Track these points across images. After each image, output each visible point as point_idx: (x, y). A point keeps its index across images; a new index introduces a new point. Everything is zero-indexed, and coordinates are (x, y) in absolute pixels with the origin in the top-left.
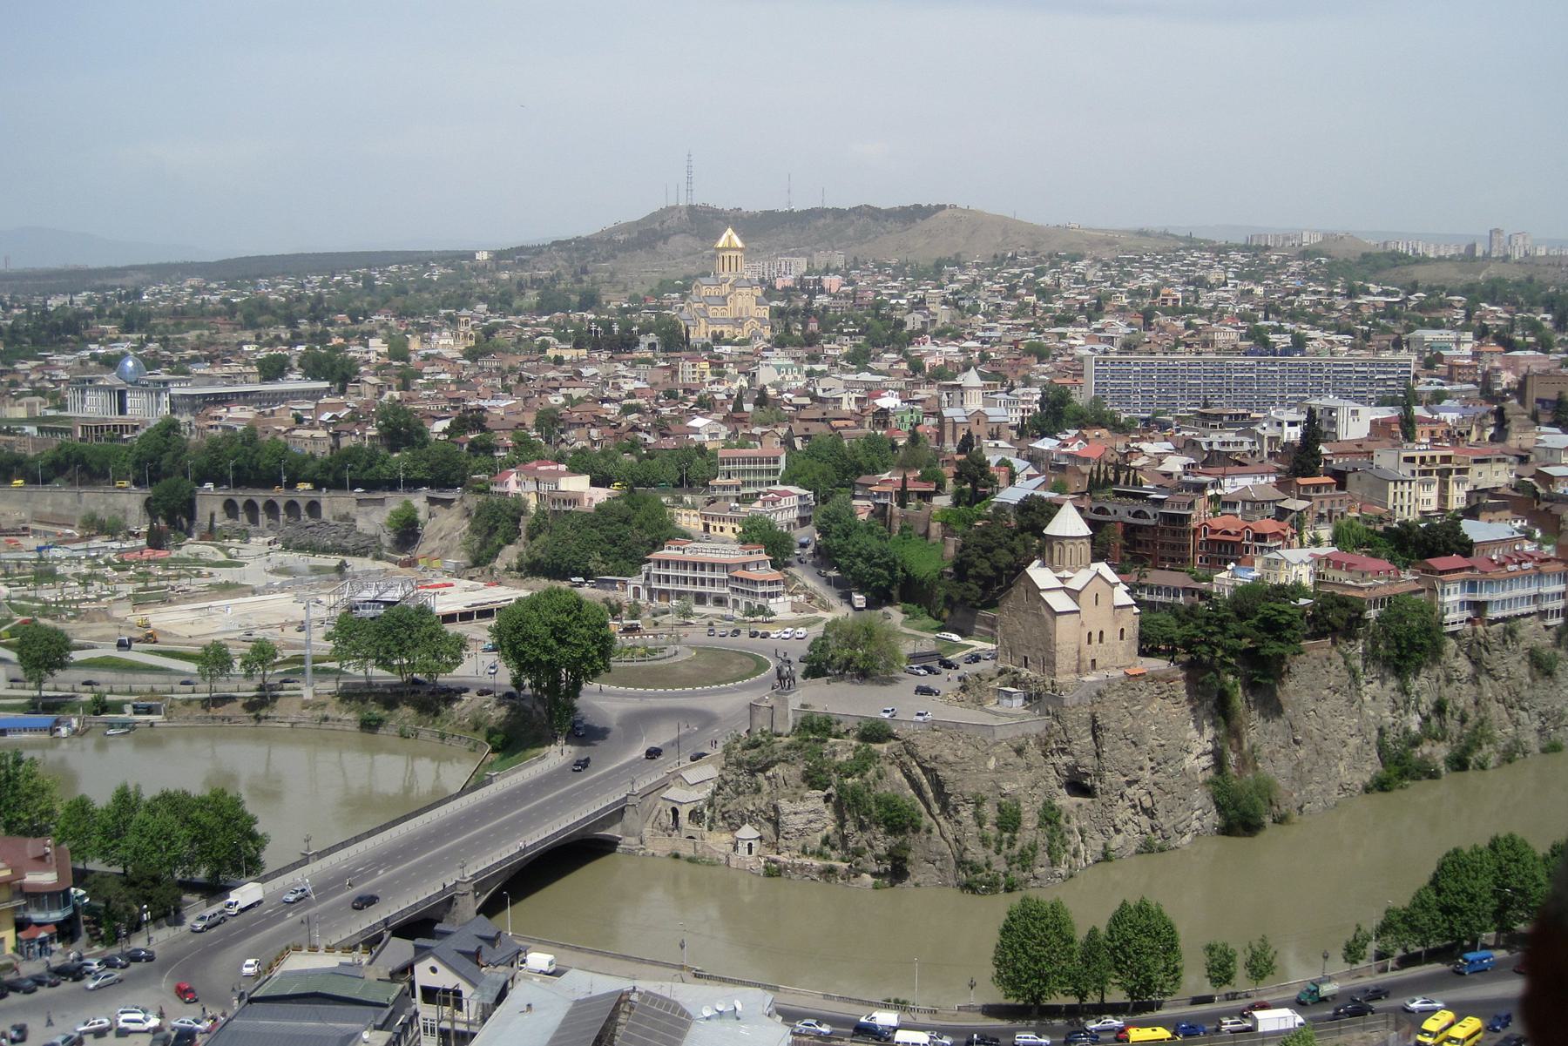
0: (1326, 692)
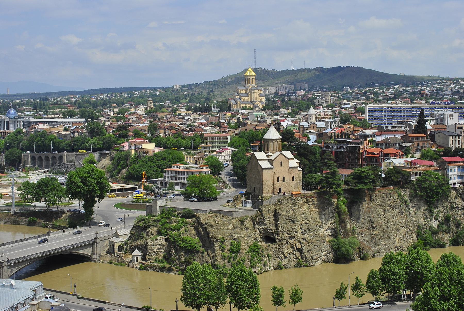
0: (388, 208)
